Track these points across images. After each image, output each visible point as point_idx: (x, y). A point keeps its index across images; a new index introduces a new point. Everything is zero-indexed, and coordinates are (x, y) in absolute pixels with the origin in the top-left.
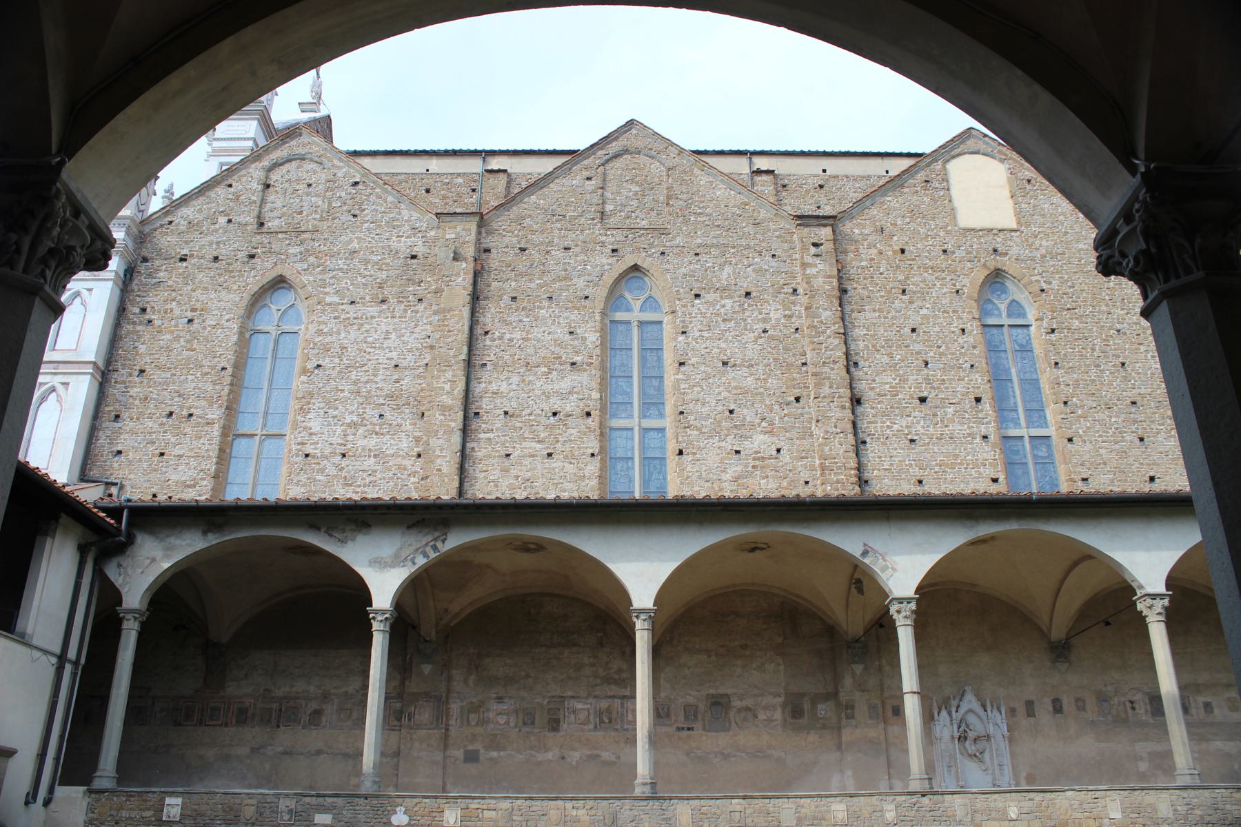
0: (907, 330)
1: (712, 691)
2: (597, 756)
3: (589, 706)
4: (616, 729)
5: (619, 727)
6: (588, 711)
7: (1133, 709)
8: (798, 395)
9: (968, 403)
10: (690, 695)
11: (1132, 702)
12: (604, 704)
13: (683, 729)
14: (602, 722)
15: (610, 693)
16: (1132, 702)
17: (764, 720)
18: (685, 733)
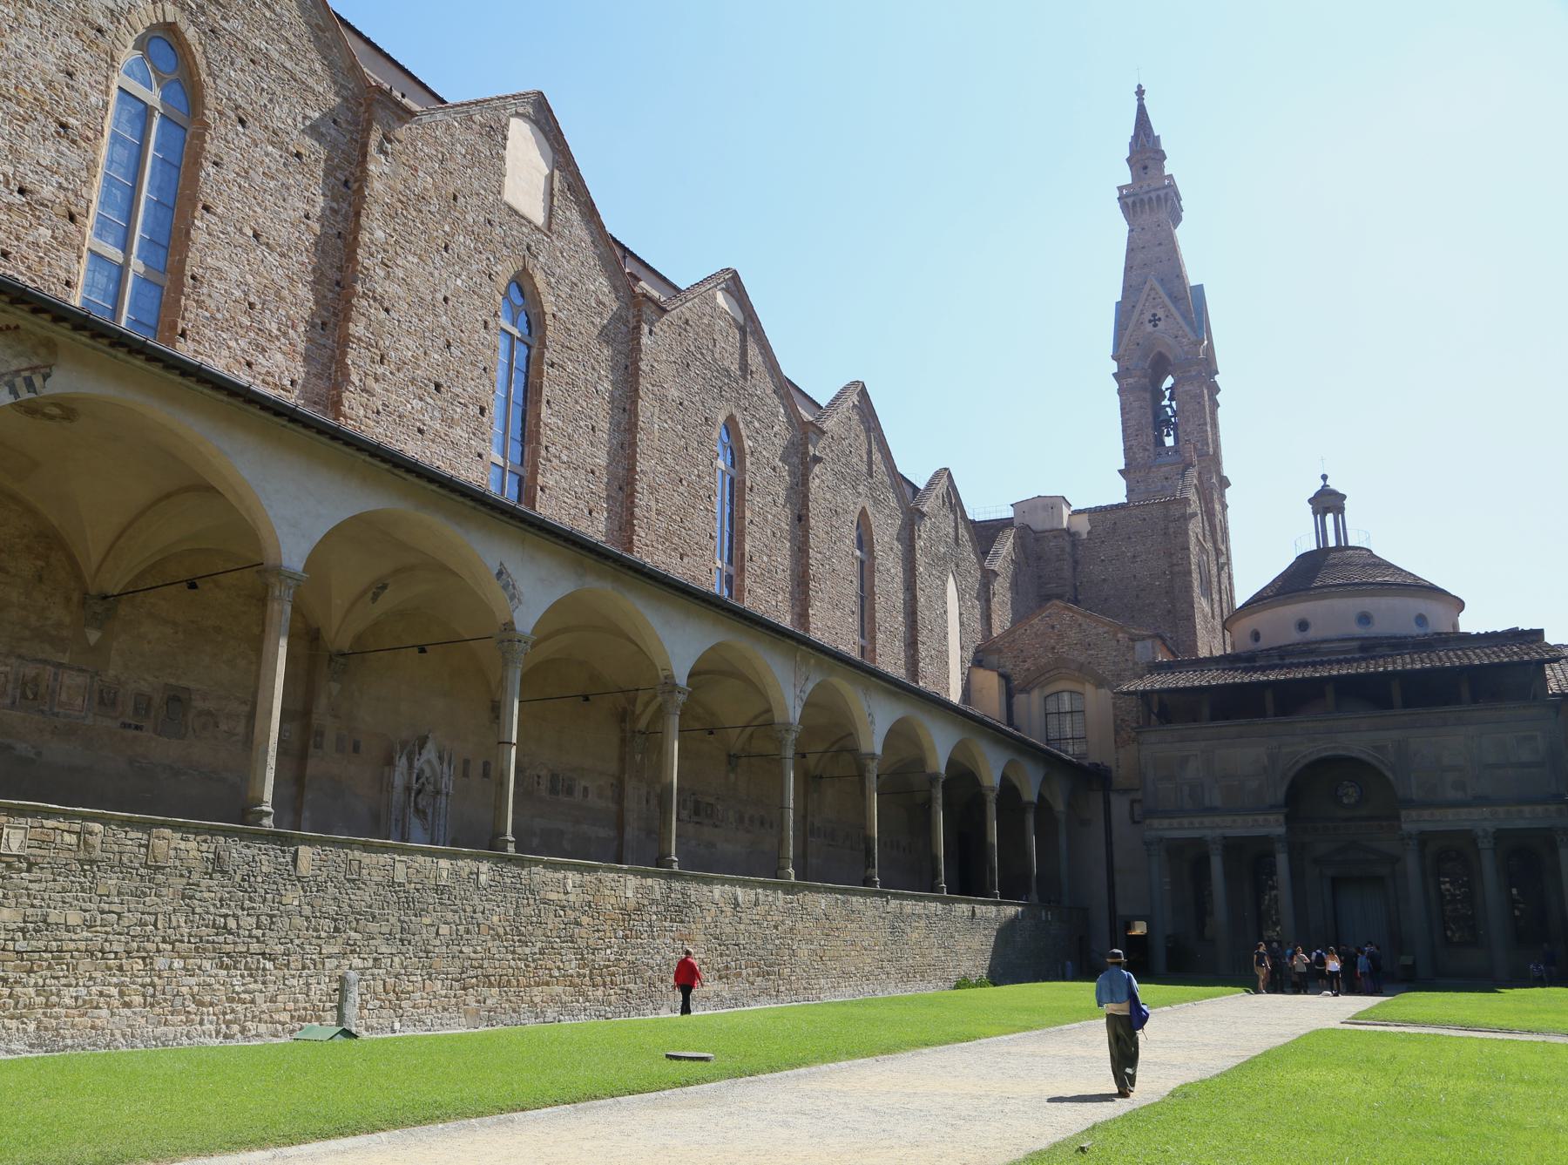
0: (440, 297)
1: (172, 681)
2: (10, 747)
3: (8, 669)
4: (43, 712)
5: (46, 708)
6: (6, 676)
7: (539, 783)
8: (326, 320)
9: (474, 410)
10: (145, 680)
11: (539, 777)
12: (30, 671)
13: (130, 726)
14: (24, 696)
15: (40, 656)
16: (539, 777)
17: (225, 732)
18: (131, 733)
